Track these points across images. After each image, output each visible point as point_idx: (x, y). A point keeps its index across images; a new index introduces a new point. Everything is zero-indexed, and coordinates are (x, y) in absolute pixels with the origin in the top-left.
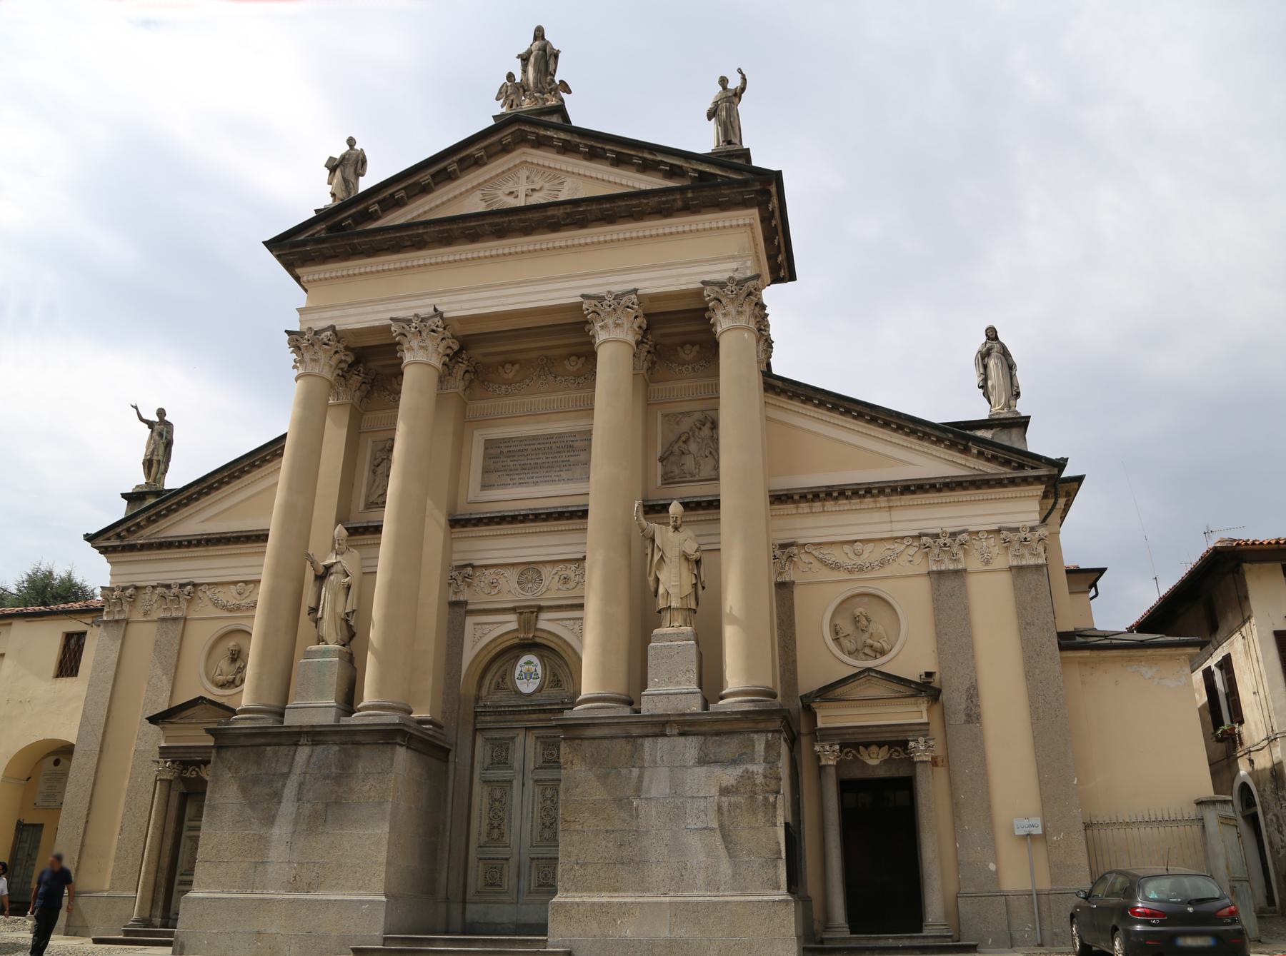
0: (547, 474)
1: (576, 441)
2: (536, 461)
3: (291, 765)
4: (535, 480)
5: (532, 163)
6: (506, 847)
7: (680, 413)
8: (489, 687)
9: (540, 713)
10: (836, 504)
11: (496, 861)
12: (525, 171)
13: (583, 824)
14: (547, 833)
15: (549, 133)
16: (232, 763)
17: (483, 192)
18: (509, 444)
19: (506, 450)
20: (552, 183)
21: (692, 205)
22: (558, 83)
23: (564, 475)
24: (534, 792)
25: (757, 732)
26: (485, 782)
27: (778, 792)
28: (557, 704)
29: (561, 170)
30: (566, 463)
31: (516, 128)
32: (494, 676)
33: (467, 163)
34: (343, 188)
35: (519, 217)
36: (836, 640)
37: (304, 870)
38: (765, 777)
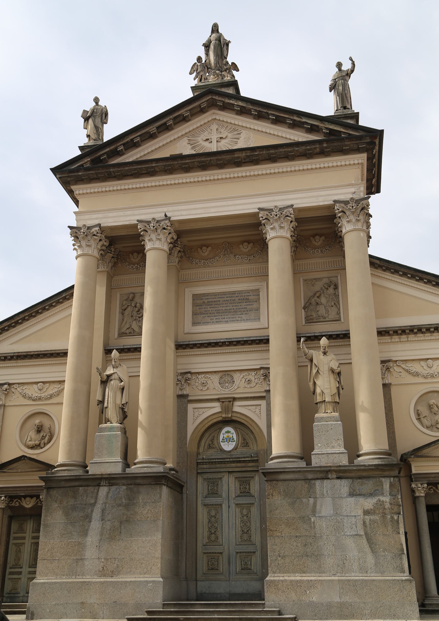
0: (233, 316)
1: (250, 296)
2: (226, 308)
3: (96, 498)
4: (226, 320)
5: (219, 120)
6: (220, 545)
7: (314, 279)
8: (204, 447)
9: (237, 463)
10: (415, 336)
11: (214, 555)
12: (215, 125)
13: (281, 532)
14: (245, 537)
15: (231, 102)
16: (58, 497)
18: (207, 297)
19: (206, 301)
20: (232, 134)
21: (326, 151)
22: (231, 64)
23: (243, 316)
24: (235, 511)
25: (384, 477)
26: (205, 505)
27: (399, 513)
28: (248, 457)
29: (239, 125)
30: (245, 310)
31: (210, 97)
32: (206, 440)
33: (178, 120)
34: (95, 131)
35: (216, 158)
36: (419, 419)
37: (109, 563)
38: (391, 504)
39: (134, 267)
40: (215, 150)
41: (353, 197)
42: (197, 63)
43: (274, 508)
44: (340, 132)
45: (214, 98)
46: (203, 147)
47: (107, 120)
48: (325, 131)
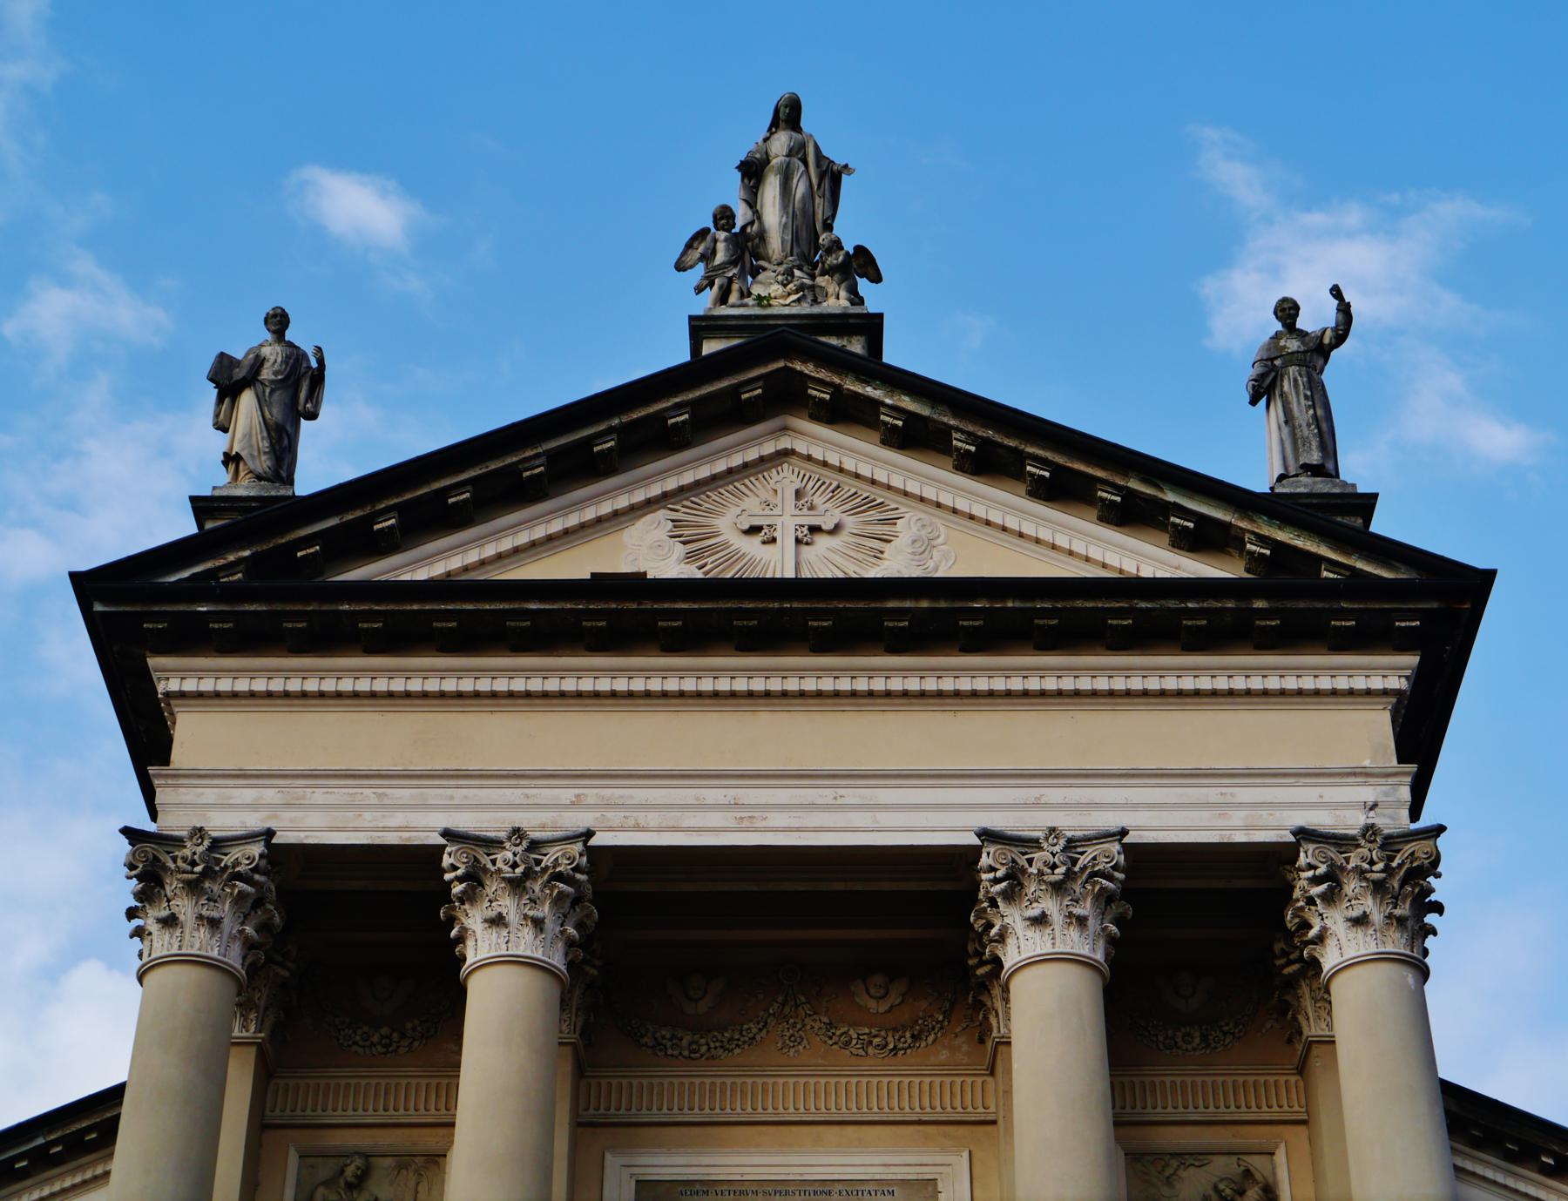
5: (809, 458)
7: (1174, 1155)
15: (869, 391)
17: (675, 516)
20: (862, 517)
22: (851, 252)
29: (889, 487)
31: (781, 364)
39: (375, 1039)
40: (794, 577)
41: (1370, 821)
42: (713, 230)
44: (1320, 559)
45: (798, 368)
46: (736, 556)
47: (317, 405)
48: (1254, 548)
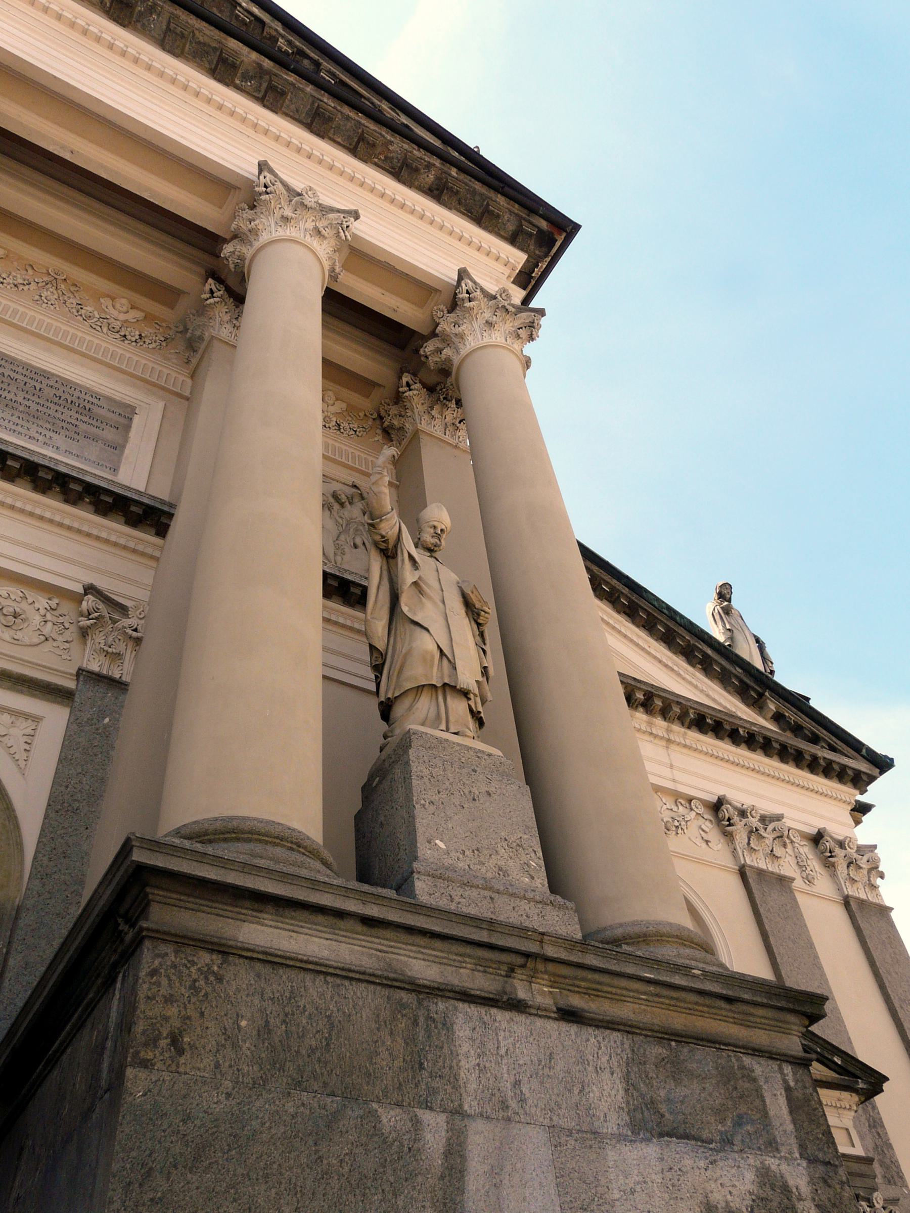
43: (177, 1148)
